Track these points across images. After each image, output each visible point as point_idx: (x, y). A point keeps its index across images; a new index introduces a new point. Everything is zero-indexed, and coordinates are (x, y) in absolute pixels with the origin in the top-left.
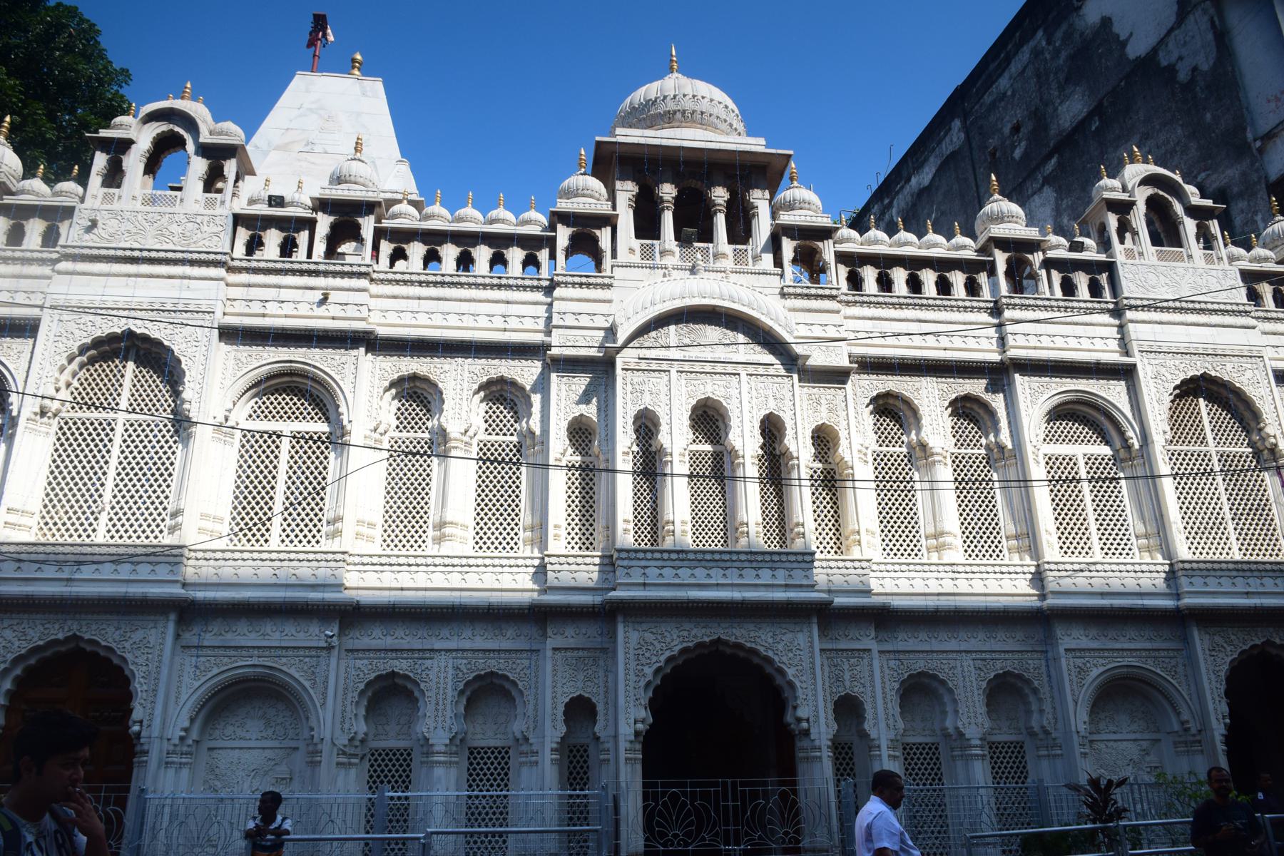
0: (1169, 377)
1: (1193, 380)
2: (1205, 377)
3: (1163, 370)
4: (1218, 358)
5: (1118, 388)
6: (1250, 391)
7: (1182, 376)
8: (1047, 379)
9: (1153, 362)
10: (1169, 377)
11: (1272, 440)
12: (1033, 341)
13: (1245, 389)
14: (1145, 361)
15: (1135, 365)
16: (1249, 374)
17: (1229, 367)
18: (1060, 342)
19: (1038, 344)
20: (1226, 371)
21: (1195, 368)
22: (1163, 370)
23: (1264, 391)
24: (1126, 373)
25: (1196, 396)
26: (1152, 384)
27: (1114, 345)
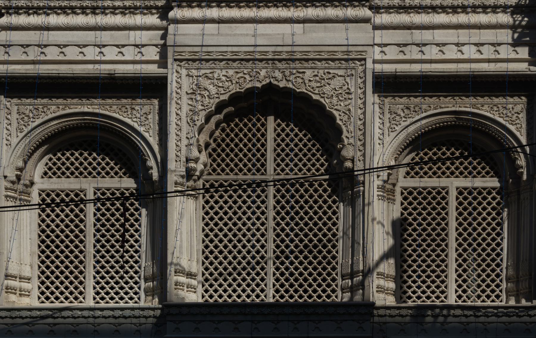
0: (213, 90)
1: (251, 91)
2: (270, 88)
3: (206, 83)
4: (298, 65)
5: (146, 109)
6: (335, 107)
7: (234, 89)
8: (45, 101)
9: (194, 72)
10: (213, 90)
11: (348, 164)
12: (33, 54)
13: (325, 102)
14: (184, 72)
15: (166, 78)
16: (337, 82)
17: (309, 73)
18: (72, 53)
19: (43, 58)
20: (306, 81)
21: (263, 76)
22: (206, 83)
23: (354, 104)
24: (153, 88)
25: (265, 115)
26: (185, 100)
27: (153, 54)
